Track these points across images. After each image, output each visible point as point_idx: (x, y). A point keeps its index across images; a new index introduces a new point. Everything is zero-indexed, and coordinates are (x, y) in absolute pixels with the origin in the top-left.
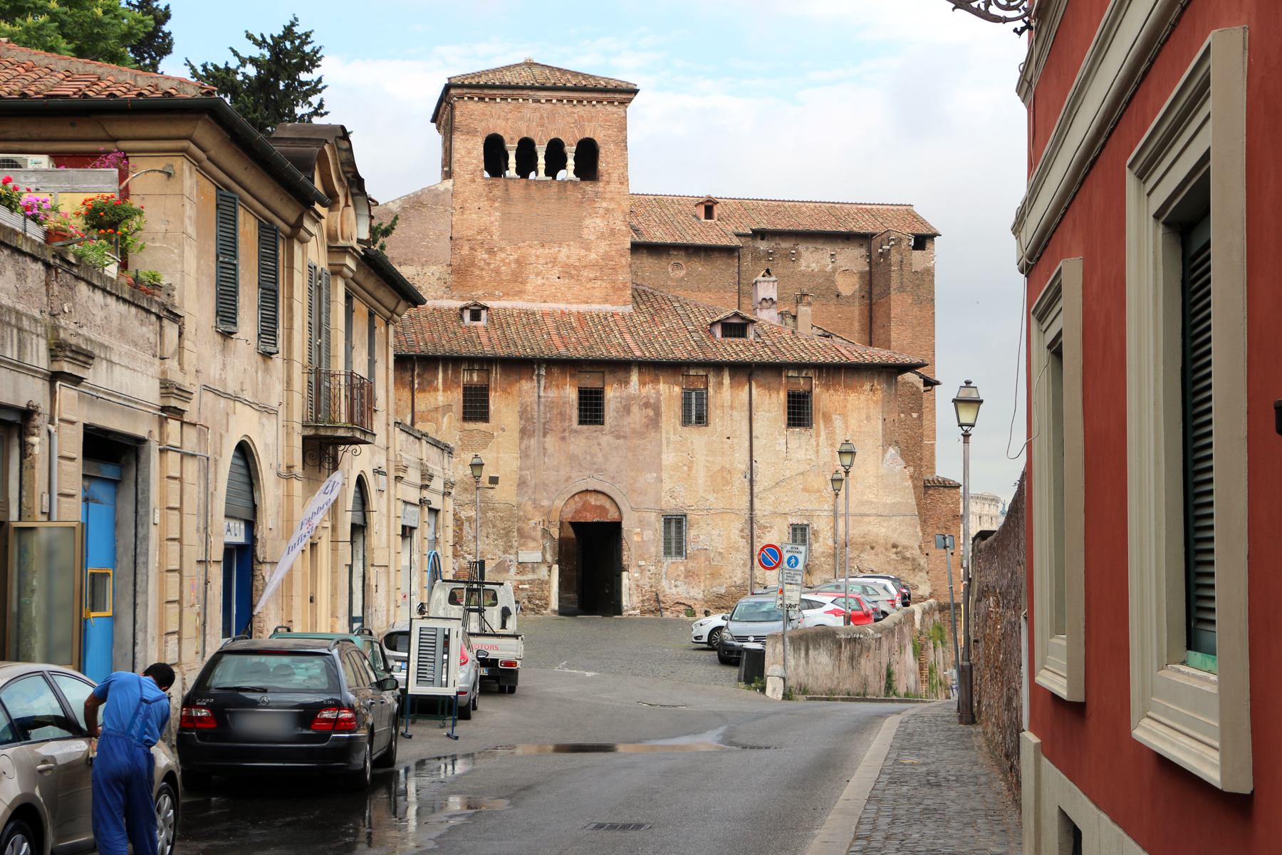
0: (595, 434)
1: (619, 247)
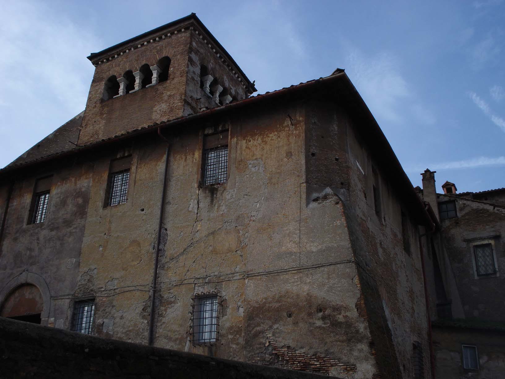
0: (36, 231)
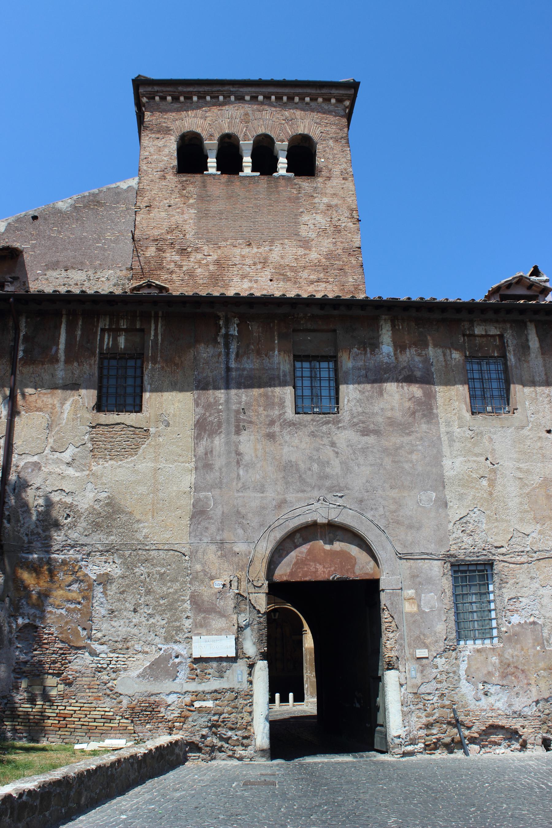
0: (324, 428)
1: (346, 245)
